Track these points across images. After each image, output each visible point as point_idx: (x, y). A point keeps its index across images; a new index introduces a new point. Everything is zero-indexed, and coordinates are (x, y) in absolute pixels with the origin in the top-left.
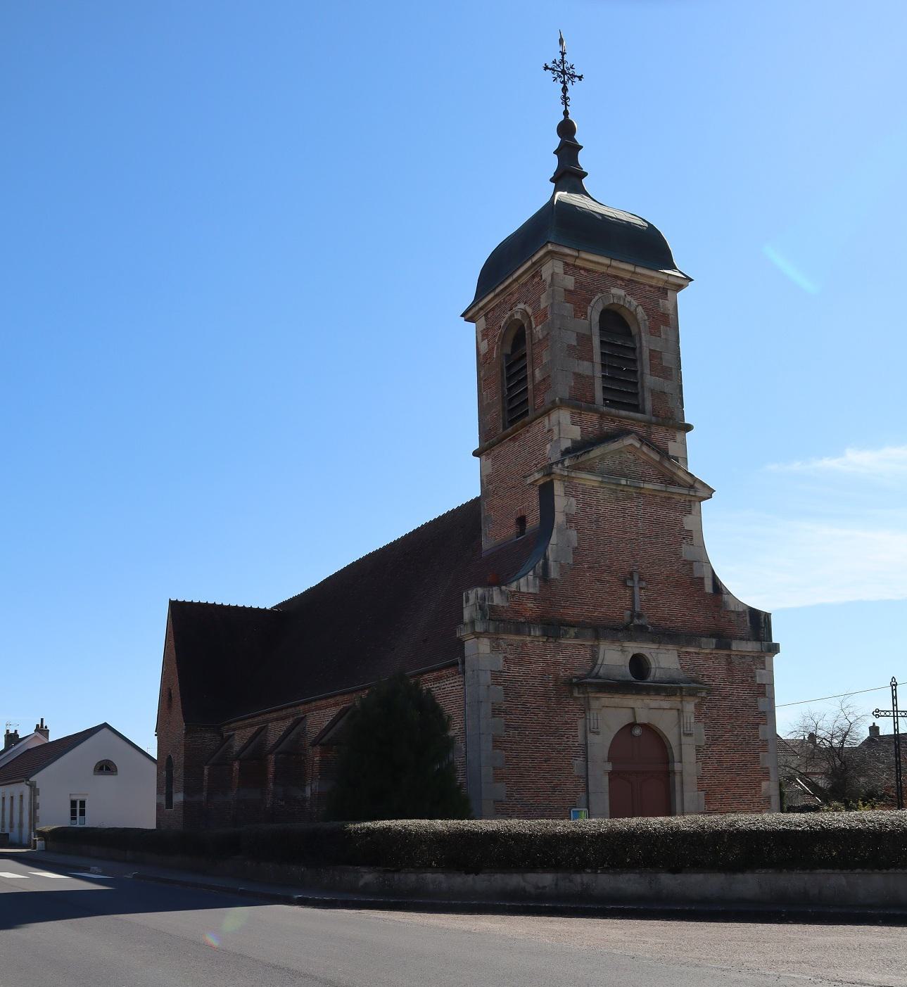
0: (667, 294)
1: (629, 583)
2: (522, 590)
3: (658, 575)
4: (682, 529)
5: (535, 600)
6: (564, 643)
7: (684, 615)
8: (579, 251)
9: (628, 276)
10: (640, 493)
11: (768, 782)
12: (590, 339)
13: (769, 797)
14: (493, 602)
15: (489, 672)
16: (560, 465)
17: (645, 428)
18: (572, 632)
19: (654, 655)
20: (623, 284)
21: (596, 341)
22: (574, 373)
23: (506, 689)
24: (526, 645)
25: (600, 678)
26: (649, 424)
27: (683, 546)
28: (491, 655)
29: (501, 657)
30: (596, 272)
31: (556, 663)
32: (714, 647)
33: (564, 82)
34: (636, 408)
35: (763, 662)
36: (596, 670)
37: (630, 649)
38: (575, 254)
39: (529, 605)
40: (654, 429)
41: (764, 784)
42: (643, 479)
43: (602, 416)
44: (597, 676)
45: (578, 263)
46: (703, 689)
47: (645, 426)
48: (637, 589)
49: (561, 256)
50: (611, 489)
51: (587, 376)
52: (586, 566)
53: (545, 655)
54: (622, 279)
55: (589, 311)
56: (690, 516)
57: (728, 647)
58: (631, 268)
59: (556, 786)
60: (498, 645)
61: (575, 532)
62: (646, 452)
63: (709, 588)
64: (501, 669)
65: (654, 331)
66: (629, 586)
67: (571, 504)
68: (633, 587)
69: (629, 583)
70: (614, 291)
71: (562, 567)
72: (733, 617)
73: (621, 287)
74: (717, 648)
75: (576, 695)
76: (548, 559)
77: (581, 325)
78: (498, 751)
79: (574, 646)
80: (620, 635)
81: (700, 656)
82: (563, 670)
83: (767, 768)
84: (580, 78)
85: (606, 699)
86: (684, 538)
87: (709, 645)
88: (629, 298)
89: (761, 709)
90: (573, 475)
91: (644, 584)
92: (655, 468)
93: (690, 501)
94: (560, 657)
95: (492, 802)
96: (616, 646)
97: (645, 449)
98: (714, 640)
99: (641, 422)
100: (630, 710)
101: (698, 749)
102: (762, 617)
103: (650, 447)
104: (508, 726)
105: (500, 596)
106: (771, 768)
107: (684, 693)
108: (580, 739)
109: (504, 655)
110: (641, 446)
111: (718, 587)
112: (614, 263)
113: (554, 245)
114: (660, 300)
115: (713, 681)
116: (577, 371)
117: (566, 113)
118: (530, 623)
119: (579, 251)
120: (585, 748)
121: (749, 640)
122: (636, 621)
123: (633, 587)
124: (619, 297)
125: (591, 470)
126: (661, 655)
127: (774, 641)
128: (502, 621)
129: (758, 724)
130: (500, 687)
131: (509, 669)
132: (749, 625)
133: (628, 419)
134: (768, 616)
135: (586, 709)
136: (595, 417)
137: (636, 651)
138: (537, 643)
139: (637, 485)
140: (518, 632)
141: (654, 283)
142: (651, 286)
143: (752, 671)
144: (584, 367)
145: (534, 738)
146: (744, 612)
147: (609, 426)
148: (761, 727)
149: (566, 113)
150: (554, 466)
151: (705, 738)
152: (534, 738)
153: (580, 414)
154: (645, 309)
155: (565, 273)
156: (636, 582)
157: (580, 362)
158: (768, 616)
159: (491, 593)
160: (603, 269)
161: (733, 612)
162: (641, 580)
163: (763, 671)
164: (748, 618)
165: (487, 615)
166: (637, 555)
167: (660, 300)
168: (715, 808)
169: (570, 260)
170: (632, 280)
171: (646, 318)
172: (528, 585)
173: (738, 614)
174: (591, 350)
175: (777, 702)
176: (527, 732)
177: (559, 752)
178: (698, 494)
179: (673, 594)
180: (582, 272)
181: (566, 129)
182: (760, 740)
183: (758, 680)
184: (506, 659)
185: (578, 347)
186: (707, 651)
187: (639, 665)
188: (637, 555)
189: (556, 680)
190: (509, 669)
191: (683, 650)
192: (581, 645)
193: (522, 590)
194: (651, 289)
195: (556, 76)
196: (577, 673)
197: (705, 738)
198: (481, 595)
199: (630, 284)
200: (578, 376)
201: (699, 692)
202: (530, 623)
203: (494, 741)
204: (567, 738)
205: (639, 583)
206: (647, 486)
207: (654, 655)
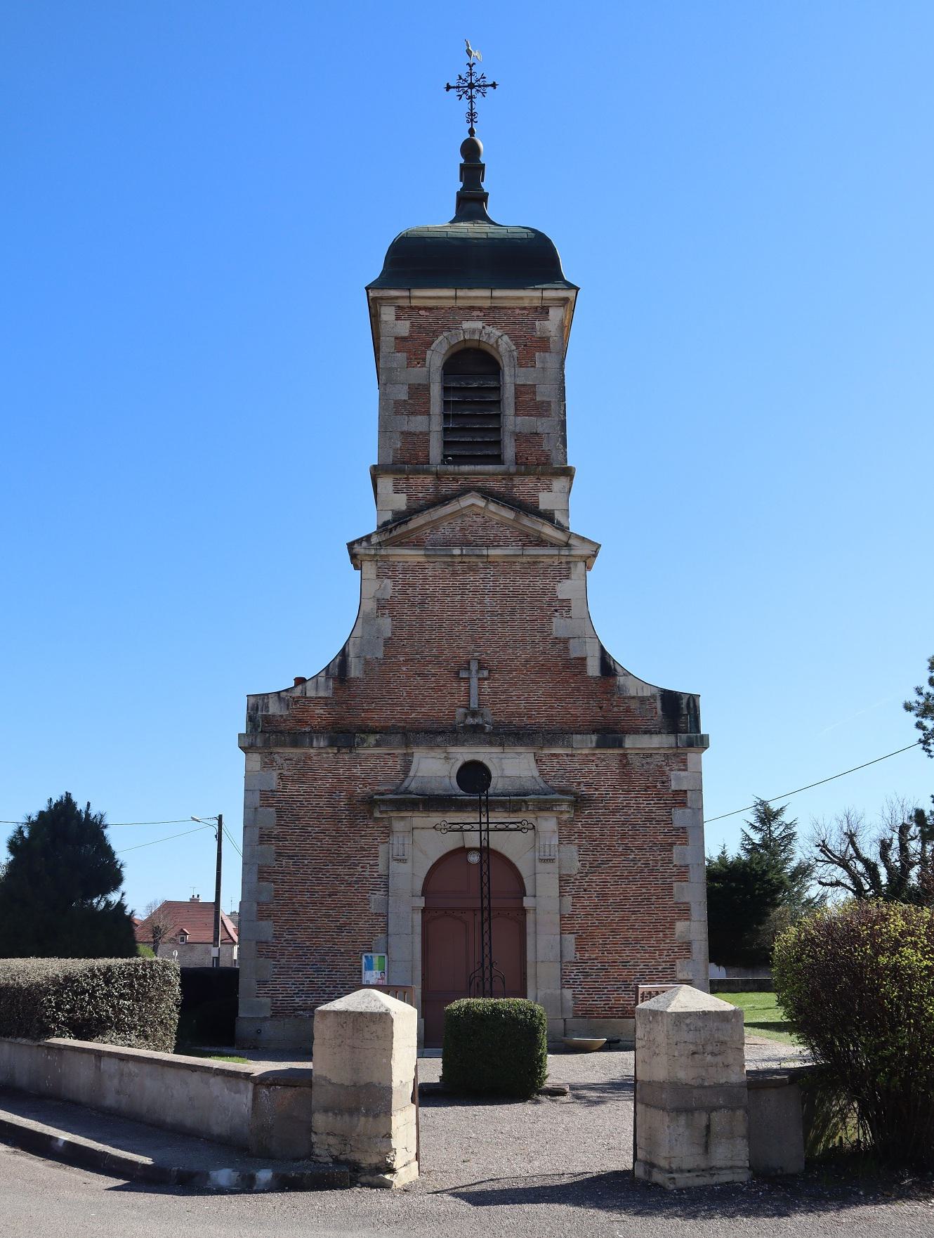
0: (548, 313)
1: (463, 674)
2: (308, 695)
3: (512, 660)
4: (555, 598)
5: (326, 705)
7: (552, 707)
8: (409, 290)
9: (487, 304)
10: (489, 562)
11: (687, 923)
12: (427, 388)
13: (689, 943)
14: (268, 711)
15: (258, 792)
16: (364, 544)
17: (504, 482)
18: (372, 739)
19: (495, 761)
20: (482, 314)
21: (436, 391)
22: (402, 433)
23: (279, 811)
24: (310, 758)
25: (410, 793)
26: (509, 476)
27: (554, 620)
28: (261, 772)
29: (275, 774)
30: (442, 309)
31: (352, 778)
32: (594, 744)
33: (471, 98)
34: (498, 459)
35: (684, 762)
36: (406, 784)
37: (459, 756)
38: (406, 294)
39: (317, 711)
40: (517, 480)
41: (680, 926)
42: (496, 544)
43: (438, 476)
44: (407, 792)
45: (414, 303)
46: (563, 801)
47: (503, 479)
48: (474, 682)
49: (390, 301)
50: (444, 562)
51: (421, 433)
52: (401, 659)
53: (337, 769)
54: (480, 309)
55: (428, 356)
56: (568, 582)
57: (620, 744)
58: (486, 293)
59: (345, 924)
60: (273, 761)
62: (494, 511)
63: (593, 669)
64: (274, 788)
65: (525, 359)
66: (462, 678)
67: (386, 585)
68: (469, 678)
69: (463, 674)
70: (467, 325)
71: (367, 663)
72: (634, 705)
73: (478, 318)
74: (598, 746)
75: (377, 814)
76: (348, 656)
77: (416, 374)
78: (265, 884)
79: (379, 757)
80: (439, 739)
81: (576, 759)
82: (361, 786)
83: (688, 903)
85: (420, 819)
86: (556, 611)
87: (585, 744)
88: (489, 329)
89: (677, 824)
90: (383, 552)
91: (486, 673)
92: (514, 528)
93: (568, 563)
94: (357, 771)
95: (254, 942)
96: (438, 753)
97: (492, 507)
98: (594, 737)
99: (497, 475)
100: (415, 830)
101: (564, 880)
102: (684, 701)
103: (498, 503)
104: (279, 854)
105: (277, 704)
106: (692, 904)
107: (530, 808)
108: (381, 868)
109: (280, 771)
110: (486, 505)
111: (608, 666)
112: (460, 293)
113: (375, 290)
114: (537, 323)
115: (597, 789)
116: (405, 428)
117: (471, 132)
118: (317, 732)
119: (409, 290)
120: (385, 882)
121: (660, 733)
122: (470, 721)
123: (469, 678)
124: (473, 331)
125: (418, 544)
126: (507, 761)
127: (703, 732)
128: (281, 732)
129: (671, 845)
130: (273, 809)
131: (284, 788)
132: (660, 712)
133: (474, 474)
134: (693, 700)
135: (388, 832)
136: (429, 480)
137: (469, 758)
138: (325, 755)
139: (477, 552)
140: (295, 744)
141: (526, 304)
142: (524, 308)
143: (663, 773)
144: (417, 424)
145: (316, 868)
146: (653, 696)
147: (447, 488)
148: (676, 849)
149: (471, 132)
150: (356, 546)
151: (579, 864)
152: (316, 868)
153: (407, 479)
154: (514, 338)
155: (398, 318)
156: (474, 672)
157: (412, 418)
158: (693, 700)
159: (266, 701)
160: (451, 303)
161: (634, 697)
162: (481, 668)
163: (683, 773)
164: (659, 704)
165: (259, 726)
166: (480, 638)
167: (537, 323)
168: (593, 956)
169: (404, 303)
170: (495, 307)
171: (514, 347)
172: (317, 689)
173: (642, 700)
174: (428, 401)
175: (707, 815)
176: (306, 861)
177: (350, 884)
178: (573, 553)
179: (533, 681)
180: (422, 312)
181: (470, 150)
182: (675, 866)
183: (674, 786)
184: (281, 777)
185: (411, 401)
186: (586, 751)
187: (475, 775)
188: (480, 638)
189: (351, 796)
190: (284, 788)
191: (546, 751)
192: (389, 754)
193: (308, 695)
194: (524, 312)
195: (461, 93)
196: (379, 788)
197: (579, 864)
198: (253, 705)
199: (491, 313)
200: (406, 435)
201: (556, 805)
202: (317, 732)
203: (260, 872)
204: (362, 867)
205: (478, 672)
206: (492, 552)
207: (495, 761)
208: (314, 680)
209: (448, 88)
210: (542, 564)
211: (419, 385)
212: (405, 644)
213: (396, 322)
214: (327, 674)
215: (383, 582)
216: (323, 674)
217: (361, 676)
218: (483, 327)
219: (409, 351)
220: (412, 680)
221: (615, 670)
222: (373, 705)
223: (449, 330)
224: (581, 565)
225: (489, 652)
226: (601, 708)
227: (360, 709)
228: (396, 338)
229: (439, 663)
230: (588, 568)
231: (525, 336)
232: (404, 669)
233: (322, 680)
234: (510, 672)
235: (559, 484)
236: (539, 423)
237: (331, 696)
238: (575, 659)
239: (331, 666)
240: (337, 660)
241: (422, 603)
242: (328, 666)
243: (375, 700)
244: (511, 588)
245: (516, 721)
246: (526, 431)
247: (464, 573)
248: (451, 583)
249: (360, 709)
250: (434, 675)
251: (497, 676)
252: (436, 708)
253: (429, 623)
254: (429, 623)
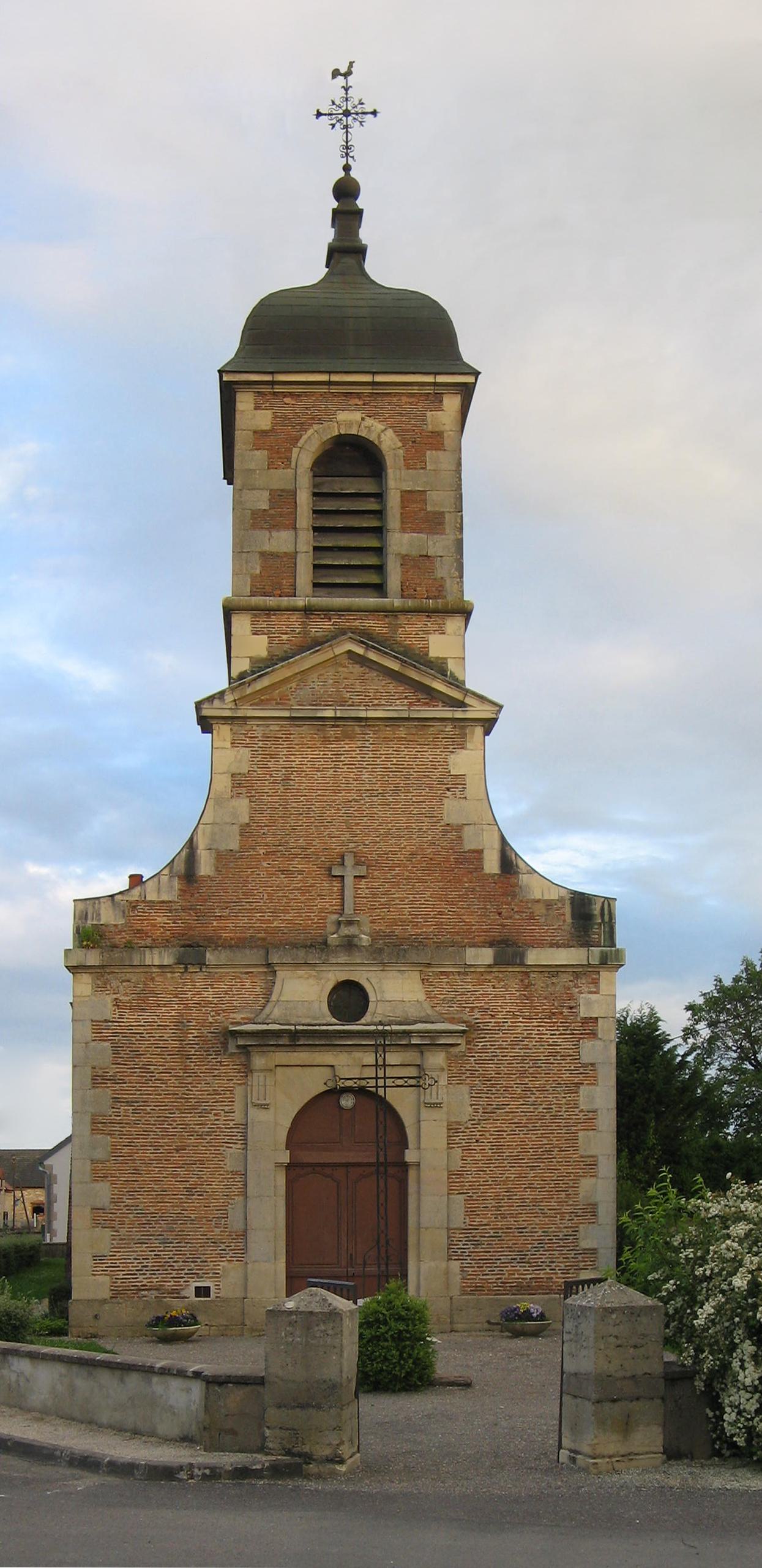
0: (441, 401)
3: (394, 853)
6: (216, 973)
11: (593, 1180)
14: (99, 920)
15: (89, 1024)
16: (217, 703)
20: (362, 402)
21: (304, 499)
22: (263, 554)
27: (445, 801)
28: (93, 998)
29: (109, 999)
33: (346, 127)
35: (596, 982)
41: (586, 1184)
42: (376, 702)
48: (349, 881)
52: (261, 852)
55: (294, 455)
61: (247, 800)
63: (491, 864)
64: (109, 1016)
65: (415, 459)
70: (342, 416)
72: (539, 910)
76: (197, 848)
77: (280, 478)
78: (99, 1136)
84: (319, 114)
86: (448, 789)
88: (369, 421)
89: (586, 1059)
101: (453, 1129)
104: (116, 1100)
106: (600, 1158)
108: (238, 1117)
109: (115, 996)
114: (429, 414)
116: (267, 548)
117: (347, 168)
124: (350, 424)
129: (578, 1085)
130: (107, 1044)
131: (121, 1016)
132: (568, 918)
137: (343, 977)
138: (169, 975)
143: (571, 997)
144: (280, 541)
145: (160, 1117)
146: (561, 900)
148: (583, 1090)
149: (347, 168)
152: (160, 1117)
154: (400, 433)
157: (274, 534)
161: (538, 901)
162: (358, 863)
163: (594, 997)
164: (567, 910)
168: (485, 1221)
171: (400, 444)
173: (549, 904)
177: (201, 1136)
179: (420, 881)
180: (287, 400)
183: (583, 1012)
184: (117, 1003)
185: (272, 512)
190: (121, 1016)
193: (148, 898)
195: (334, 122)
204: (215, 1115)
208: (155, 879)
210: (432, 729)
211: (282, 491)
212: (266, 831)
213: (255, 412)
214: (171, 872)
215: (238, 751)
216: (166, 872)
217: (211, 874)
218: (363, 419)
219: (270, 449)
220: (274, 879)
221: (517, 866)
222: (227, 911)
223: (320, 421)
224: (479, 731)
225: (367, 842)
226: (500, 914)
227: (212, 916)
228: (255, 432)
229: (306, 856)
230: (487, 732)
231: (414, 430)
232: (265, 864)
233: (164, 879)
234: (392, 868)
235: (453, 624)
236: (430, 543)
237: (176, 900)
238: (469, 851)
239: (176, 860)
240: (184, 854)
241: (287, 779)
242: (173, 861)
243: (229, 905)
244: (395, 760)
245: (398, 930)
246: (413, 553)
247: (338, 739)
248: (322, 753)
249: (212, 916)
250: (301, 872)
251: (376, 873)
252: (304, 915)
253: (294, 805)
254: (294, 805)
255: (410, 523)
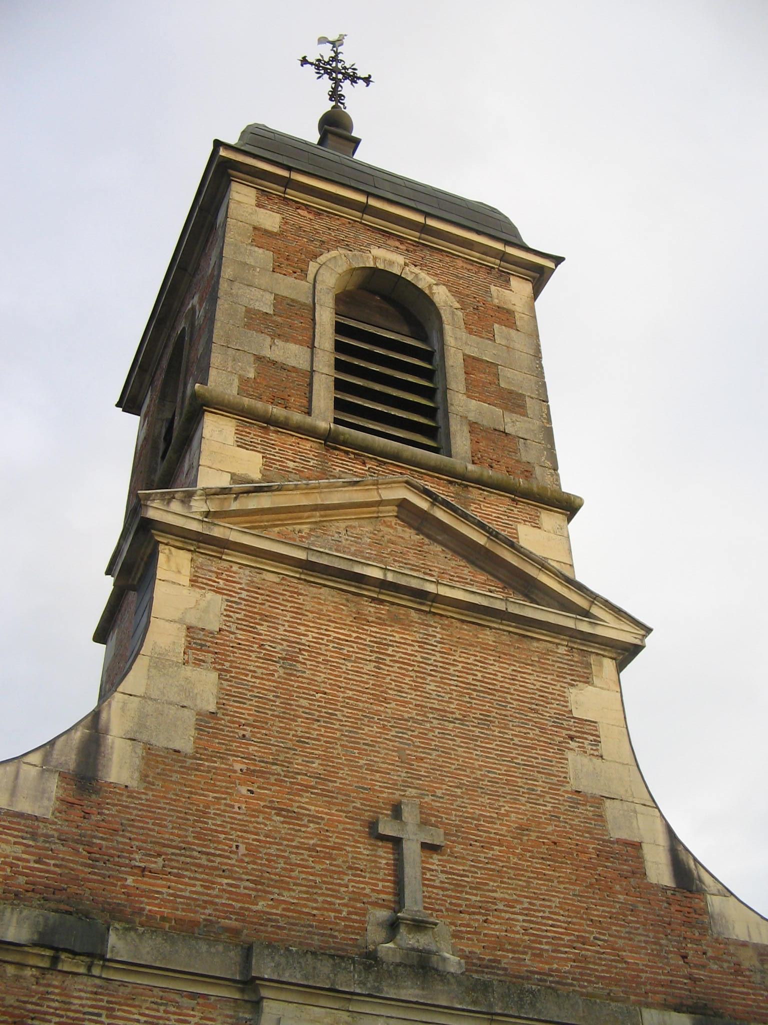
6: (123, 984)
21: (326, 317)
22: (259, 358)
27: (570, 755)
52: (238, 767)
61: (215, 675)
70: (376, 251)
76: (107, 731)
86: (572, 738)
116: (267, 353)
161: (744, 944)
162: (424, 823)
171: (458, 305)
192: (193, 996)
208: (10, 768)
209: (304, 61)
210: (535, 644)
211: (293, 300)
212: (248, 734)
213: (258, 209)
214: (46, 760)
215: (204, 595)
216: (36, 758)
217: (134, 784)
218: (406, 264)
219: (277, 252)
220: (260, 820)
221: (701, 881)
222: (160, 860)
223: (347, 247)
224: (609, 665)
225: (439, 793)
226: (684, 957)
227: (126, 866)
228: (255, 228)
229: (325, 793)
230: (621, 666)
231: (475, 298)
232: (244, 790)
233: (30, 773)
234: (487, 845)
235: (550, 519)
236: (507, 420)
237: (49, 816)
238: (618, 841)
239: (59, 744)
240: (77, 735)
241: (289, 659)
242: (52, 743)
243: (165, 849)
244: (479, 674)
245: (507, 959)
246: (485, 423)
247: (381, 622)
248: (354, 635)
249: (126, 866)
250: (314, 819)
251: (458, 848)
252: (320, 899)
253: (304, 703)
254: (304, 703)
255: (470, 392)
